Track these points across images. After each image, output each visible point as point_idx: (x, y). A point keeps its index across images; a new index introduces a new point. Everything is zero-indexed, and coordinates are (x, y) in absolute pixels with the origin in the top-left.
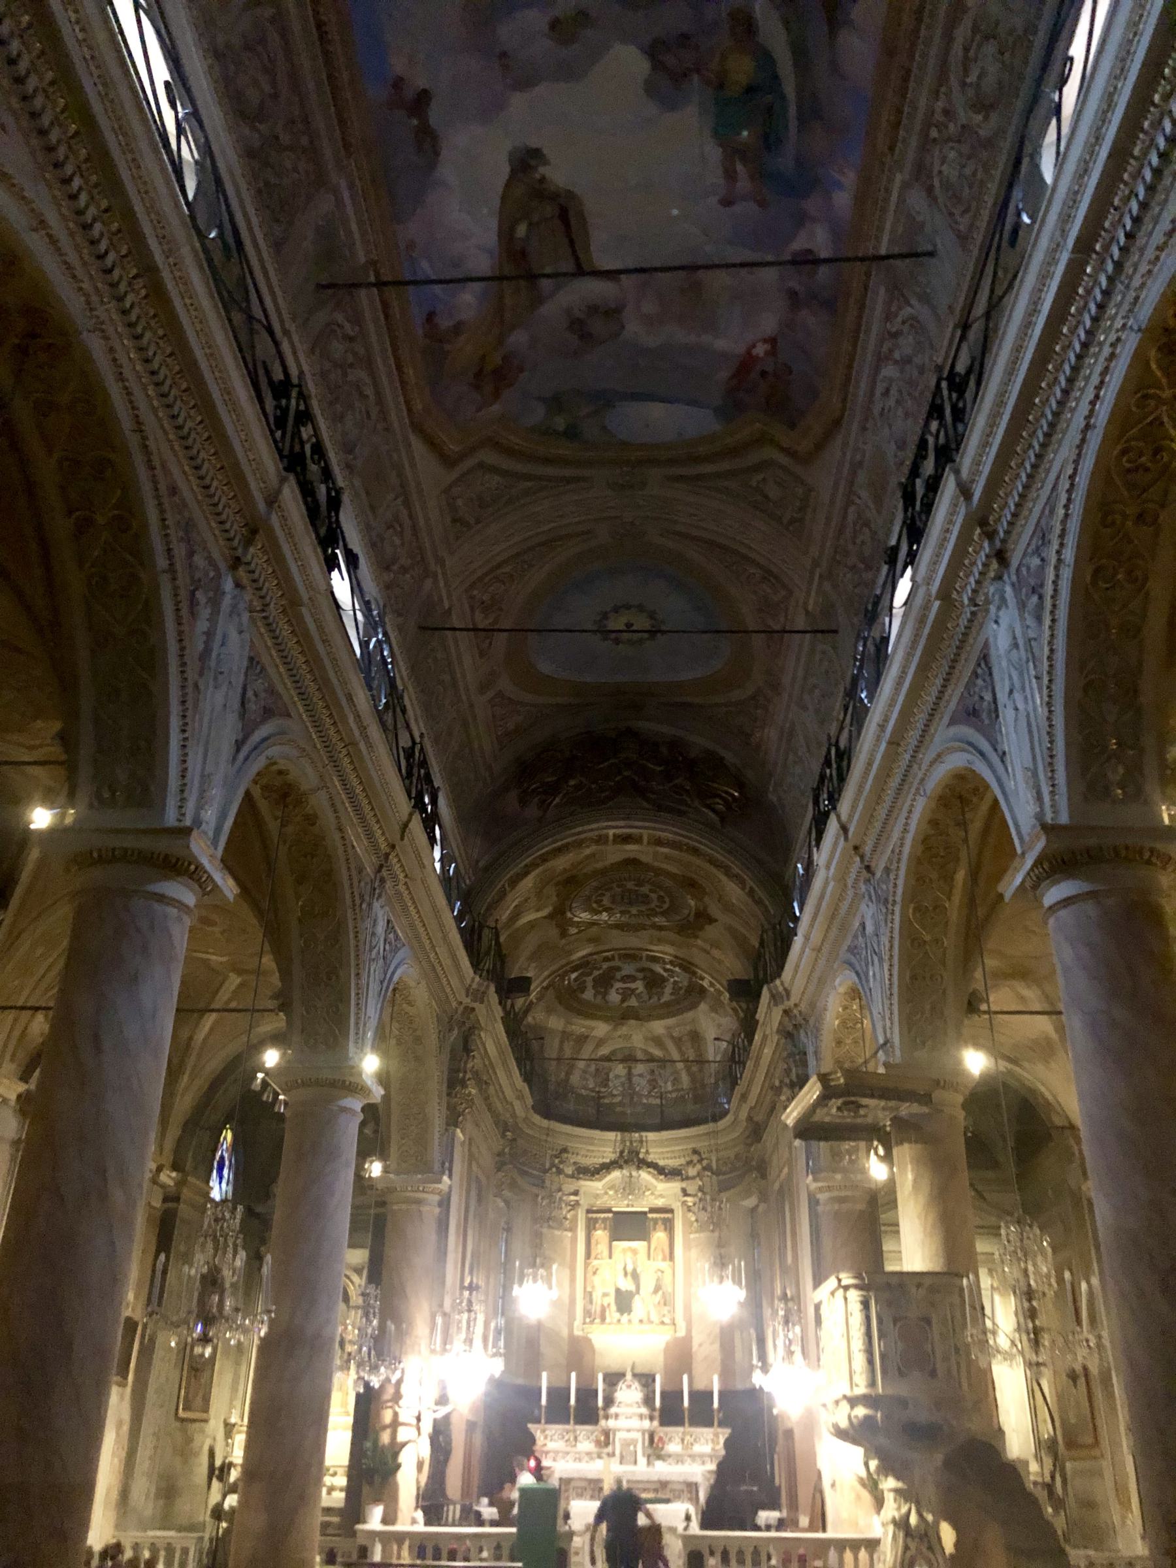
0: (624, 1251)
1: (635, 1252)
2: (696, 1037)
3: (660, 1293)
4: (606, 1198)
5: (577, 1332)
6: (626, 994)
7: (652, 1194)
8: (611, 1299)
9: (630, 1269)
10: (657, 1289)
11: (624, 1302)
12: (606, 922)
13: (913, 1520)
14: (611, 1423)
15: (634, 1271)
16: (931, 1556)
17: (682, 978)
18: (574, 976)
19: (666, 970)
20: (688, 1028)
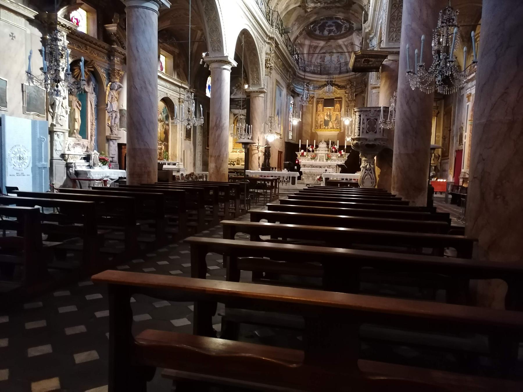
0: (327, 109)
1: (330, 110)
2: (352, 44)
4: (322, 95)
5: (313, 131)
6: (330, 31)
7: (336, 93)
8: (323, 123)
9: (328, 114)
10: (336, 119)
11: (326, 123)
12: (320, 7)
13: (368, 167)
14: (317, 152)
15: (330, 114)
16: (371, 174)
17: (348, 25)
18: (312, 26)
19: (342, 22)
20: (350, 41)
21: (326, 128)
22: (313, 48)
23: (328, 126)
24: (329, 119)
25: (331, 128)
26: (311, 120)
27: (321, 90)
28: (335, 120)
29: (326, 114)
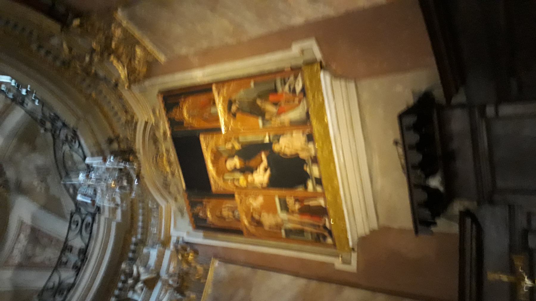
0: (221, 172)
1: (217, 156)
3: (259, 102)
9: (236, 162)
21: (315, 171)
22: (38, 250)
23: (303, 162)
24: (264, 156)
25: (310, 138)
26: (286, 279)
27: (158, 205)
28: (261, 113)
29: (242, 180)
